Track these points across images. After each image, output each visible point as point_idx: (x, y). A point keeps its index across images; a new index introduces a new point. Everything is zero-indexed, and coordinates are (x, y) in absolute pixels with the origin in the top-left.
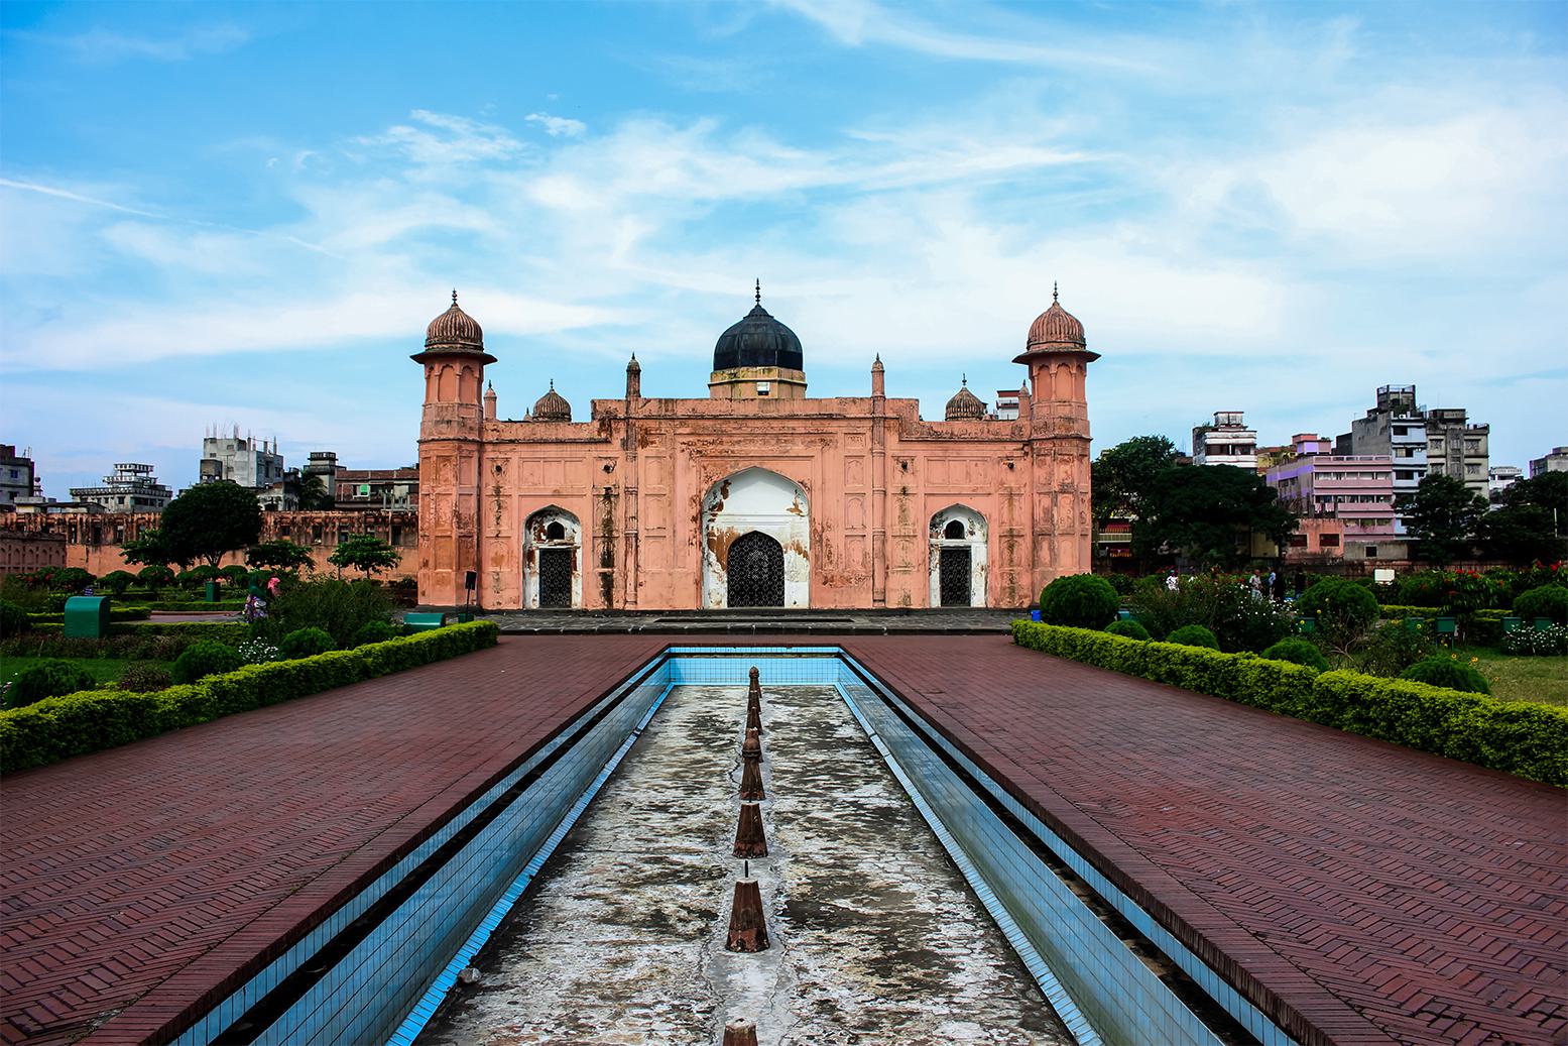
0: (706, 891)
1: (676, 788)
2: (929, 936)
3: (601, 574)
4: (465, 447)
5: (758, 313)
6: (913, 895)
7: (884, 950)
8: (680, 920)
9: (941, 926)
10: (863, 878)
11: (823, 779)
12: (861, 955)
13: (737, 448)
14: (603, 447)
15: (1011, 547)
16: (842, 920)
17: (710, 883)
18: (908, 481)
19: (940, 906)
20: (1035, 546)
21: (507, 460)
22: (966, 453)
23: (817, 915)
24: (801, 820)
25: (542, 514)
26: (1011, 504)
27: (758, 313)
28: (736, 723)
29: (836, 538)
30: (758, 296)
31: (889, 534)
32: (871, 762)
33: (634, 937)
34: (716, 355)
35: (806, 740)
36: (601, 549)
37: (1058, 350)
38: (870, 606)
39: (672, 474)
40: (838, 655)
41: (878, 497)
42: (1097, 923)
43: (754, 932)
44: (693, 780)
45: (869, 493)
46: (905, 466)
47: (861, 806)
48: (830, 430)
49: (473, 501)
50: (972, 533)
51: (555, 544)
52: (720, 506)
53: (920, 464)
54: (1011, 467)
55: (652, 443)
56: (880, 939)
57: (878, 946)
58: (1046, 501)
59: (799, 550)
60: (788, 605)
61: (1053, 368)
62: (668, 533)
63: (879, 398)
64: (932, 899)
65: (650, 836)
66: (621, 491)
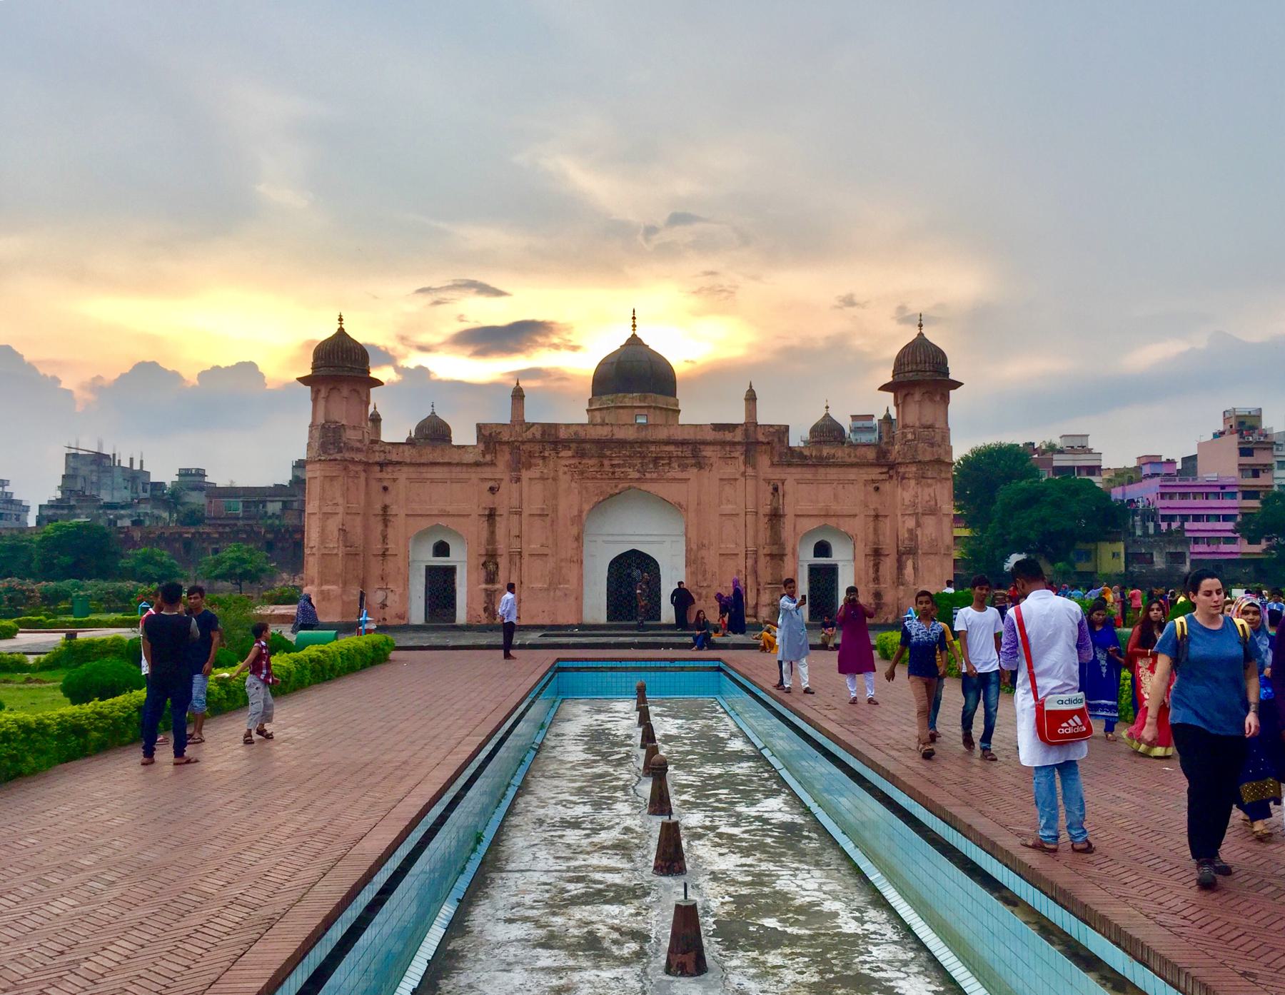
0: (633, 911)
1: (584, 803)
2: (861, 958)
3: (486, 590)
4: (351, 467)
5: (634, 341)
6: (835, 915)
7: (821, 972)
8: (615, 942)
9: (871, 948)
10: (785, 896)
11: (723, 793)
12: (799, 978)
14: (488, 469)
16: (772, 940)
17: (636, 903)
19: (866, 926)
21: (395, 480)
22: (835, 477)
23: (747, 935)
24: (711, 835)
27: (634, 341)
28: (629, 737)
29: (711, 558)
30: (634, 326)
31: (761, 552)
32: (766, 775)
33: (571, 963)
35: (699, 754)
37: (922, 374)
40: (719, 669)
42: (1053, 954)
43: (693, 955)
44: (599, 793)
47: (766, 821)
51: (441, 561)
53: (789, 487)
54: (877, 489)
55: (536, 465)
56: (814, 962)
57: (813, 969)
58: (911, 523)
61: (917, 397)
63: (751, 424)
64: (855, 918)
65: (567, 853)
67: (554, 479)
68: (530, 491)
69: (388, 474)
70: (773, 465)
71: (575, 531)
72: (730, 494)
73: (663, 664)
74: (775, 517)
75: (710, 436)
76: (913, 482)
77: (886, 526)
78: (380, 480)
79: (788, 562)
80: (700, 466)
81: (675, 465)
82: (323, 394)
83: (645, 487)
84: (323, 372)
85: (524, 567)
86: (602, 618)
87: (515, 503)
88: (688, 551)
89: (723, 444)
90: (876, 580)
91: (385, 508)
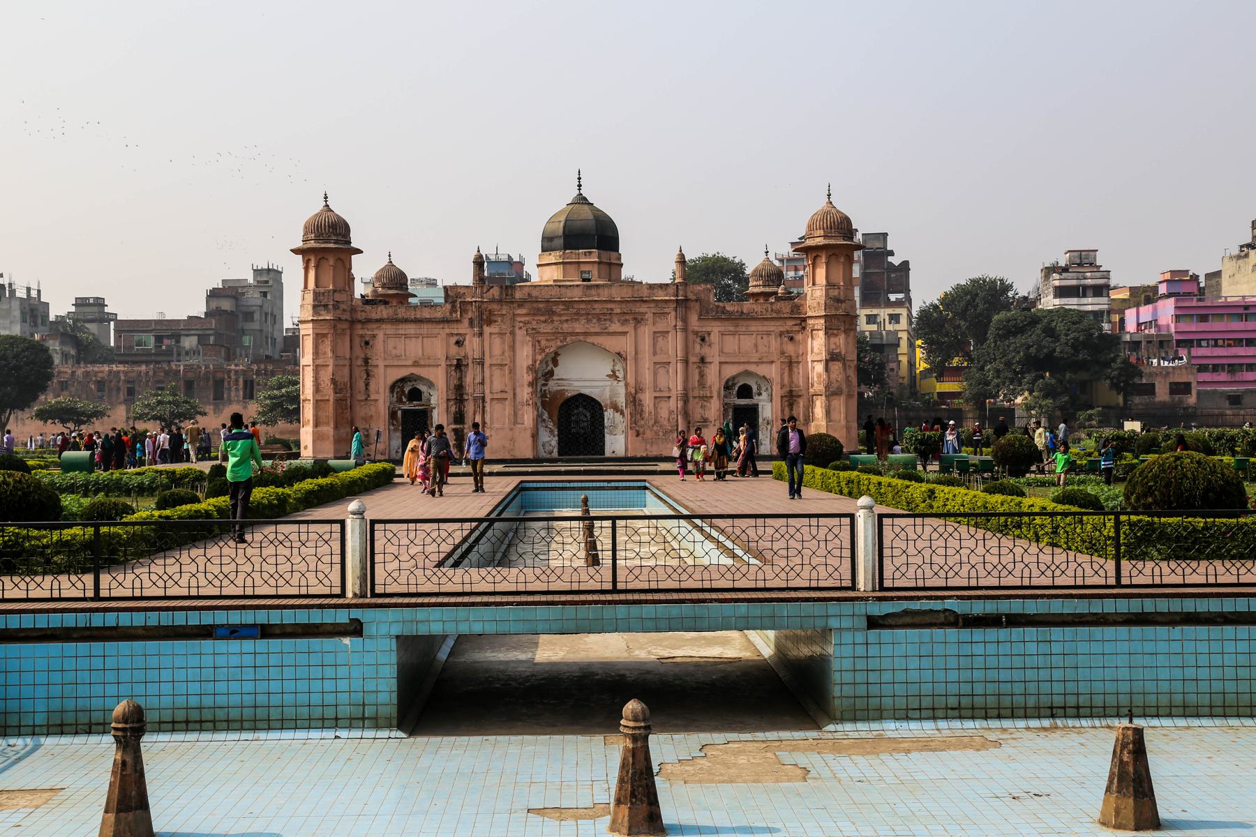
4: (340, 326)
5: (581, 200)
13: (565, 326)
15: (791, 405)
18: (706, 350)
22: (753, 329)
25: (403, 380)
26: (791, 370)
29: (647, 398)
30: (580, 186)
31: (691, 394)
34: (543, 238)
36: (453, 409)
39: (513, 348)
40: (646, 488)
45: (673, 361)
46: (703, 340)
48: (642, 310)
49: (346, 371)
50: (760, 394)
52: (551, 373)
53: (714, 337)
54: (791, 339)
59: (616, 408)
60: (608, 454)
62: (510, 396)
66: (470, 361)
67: (513, 333)
70: (700, 319)
73: (602, 484)
76: (821, 333)
78: (362, 336)
81: (615, 319)
82: (312, 264)
83: (590, 339)
84: (312, 244)
85: (488, 408)
86: (555, 454)
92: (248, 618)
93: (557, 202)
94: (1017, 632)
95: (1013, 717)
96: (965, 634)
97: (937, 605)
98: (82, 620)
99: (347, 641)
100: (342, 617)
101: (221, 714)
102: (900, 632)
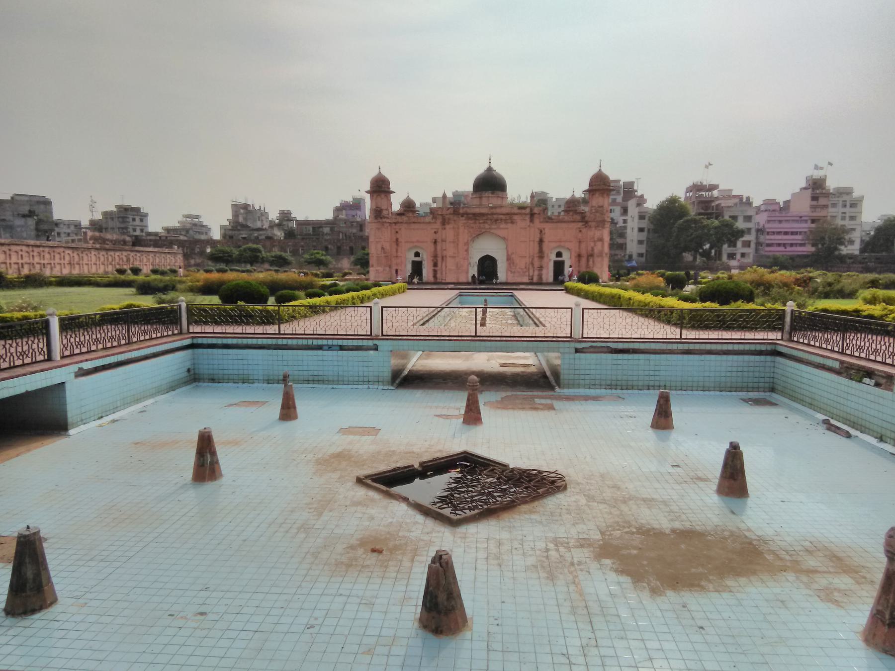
5: (490, 169)
15: (579, 261)
20: (588, 261)
38: (528, 281)
41: (532, 243)
53: (547, 231)
58: (592, 244)
61: (597, 195)
68: (449, 233)
69: (397, 226)
71: (466, 248)
72: (523, 233)
74: (541, 241)
75: (516, 210)
77: (583, 245)
79: (545, 260)
80: (512, 223)
83: (492, 231)
87: (444, 237)
88: (508, 255)
89: (520, 214)
90: (579, 266)
91: (397, 239)
92: (335, 342)
93: (479, 170)
94: (636, 356)
95: (632, 389)
96: (615, 356)
97: (604, 345)
98: (274, 342)
99: (372, 352)
100: (370, 343)
101: (326, 378)
102: (588, 355)
